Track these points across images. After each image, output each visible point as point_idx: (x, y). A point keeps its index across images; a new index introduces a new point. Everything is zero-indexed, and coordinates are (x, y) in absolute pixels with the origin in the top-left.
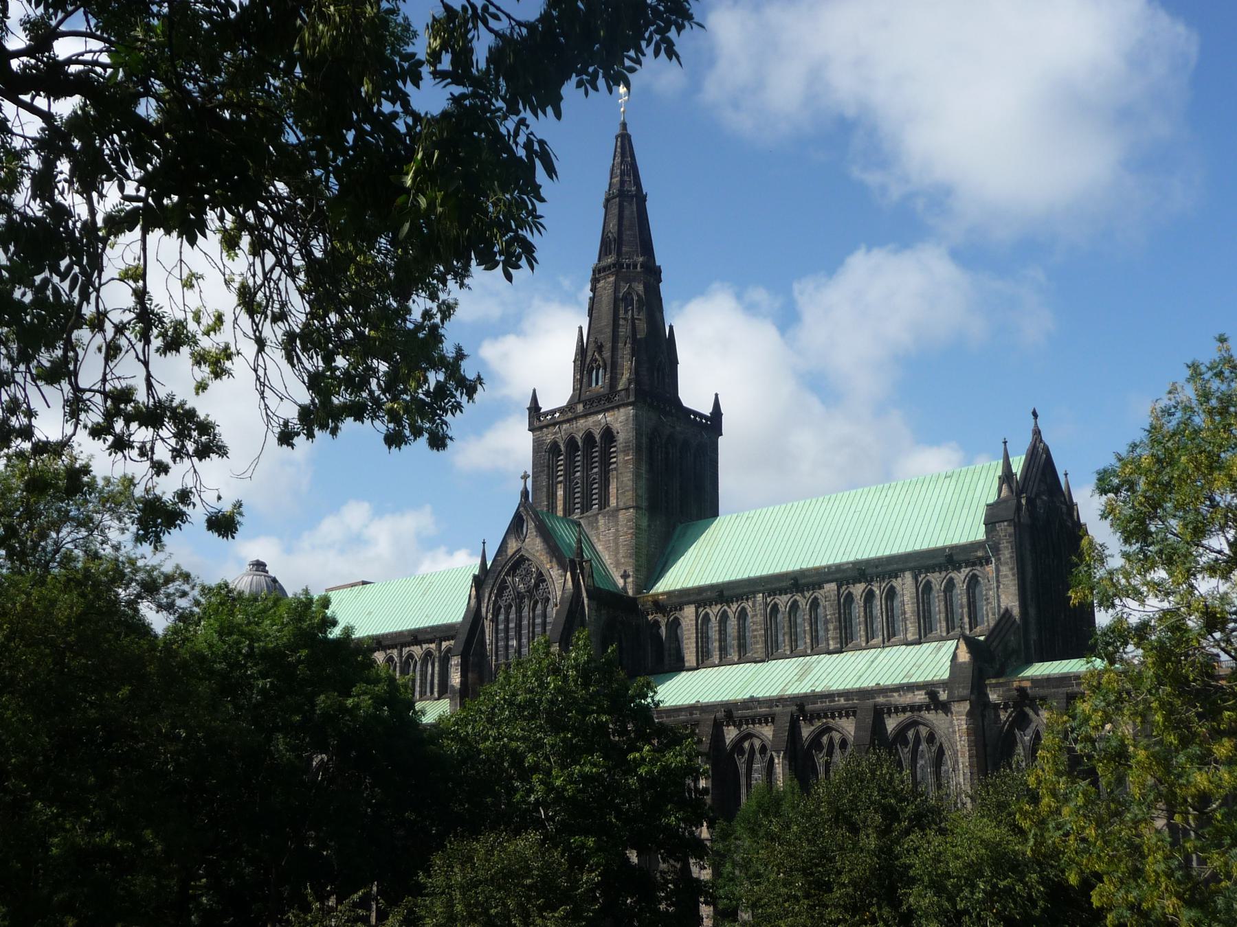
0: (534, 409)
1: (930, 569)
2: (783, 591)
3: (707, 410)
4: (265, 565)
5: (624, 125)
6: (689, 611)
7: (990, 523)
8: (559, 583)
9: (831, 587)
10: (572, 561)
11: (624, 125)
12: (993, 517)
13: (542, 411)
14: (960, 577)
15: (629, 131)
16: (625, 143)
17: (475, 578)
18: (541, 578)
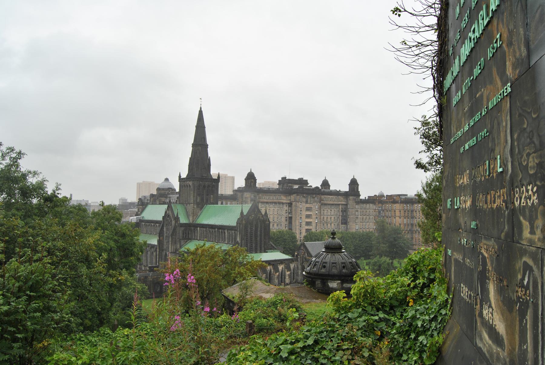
0: (180, 176)
1: (229, 230)
2: (210, 228)
3: (215, 177)
4: (168, 179)
5: (201, 108)
6: (198, 228)
7: (237, 223)
8: (173, 222)
9: (216, 229)
10: (175, 218)
11: (201, 108)
12: (239, 221)
13: (181, 178)
14: (233, 232)
15: (202, 110)
16: (201, 113)
17: (163, 217)
18: (171, 221)
